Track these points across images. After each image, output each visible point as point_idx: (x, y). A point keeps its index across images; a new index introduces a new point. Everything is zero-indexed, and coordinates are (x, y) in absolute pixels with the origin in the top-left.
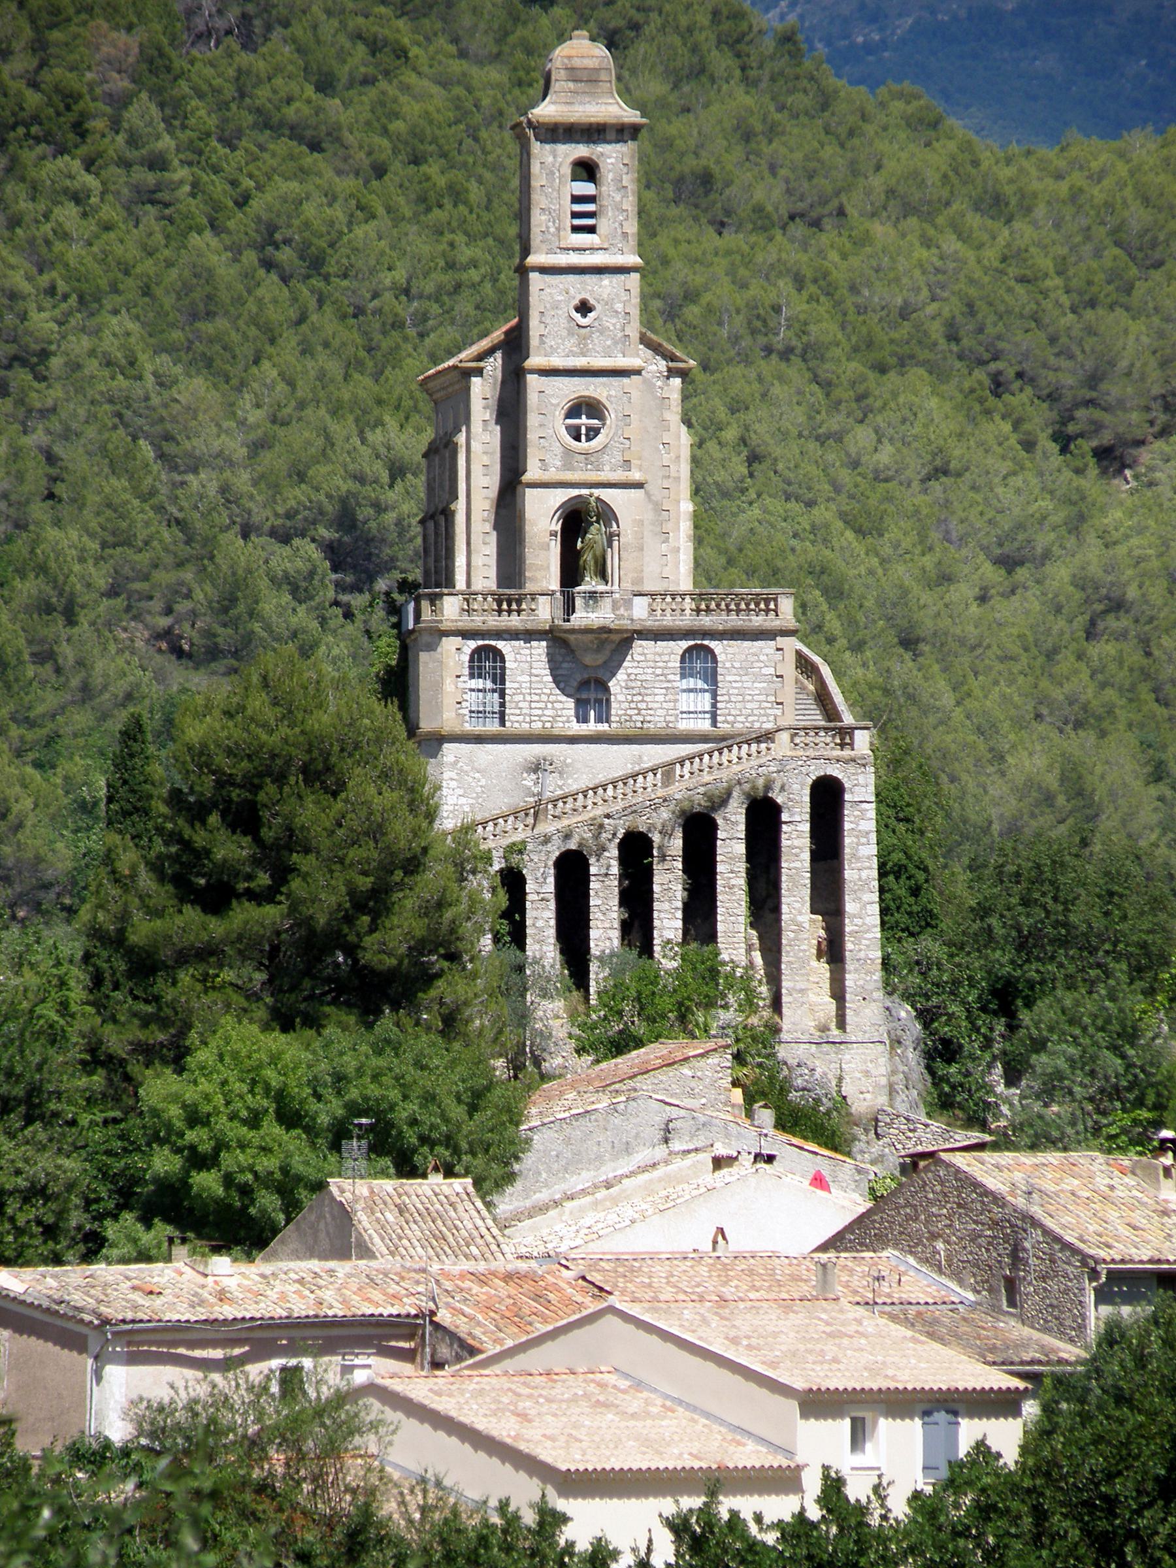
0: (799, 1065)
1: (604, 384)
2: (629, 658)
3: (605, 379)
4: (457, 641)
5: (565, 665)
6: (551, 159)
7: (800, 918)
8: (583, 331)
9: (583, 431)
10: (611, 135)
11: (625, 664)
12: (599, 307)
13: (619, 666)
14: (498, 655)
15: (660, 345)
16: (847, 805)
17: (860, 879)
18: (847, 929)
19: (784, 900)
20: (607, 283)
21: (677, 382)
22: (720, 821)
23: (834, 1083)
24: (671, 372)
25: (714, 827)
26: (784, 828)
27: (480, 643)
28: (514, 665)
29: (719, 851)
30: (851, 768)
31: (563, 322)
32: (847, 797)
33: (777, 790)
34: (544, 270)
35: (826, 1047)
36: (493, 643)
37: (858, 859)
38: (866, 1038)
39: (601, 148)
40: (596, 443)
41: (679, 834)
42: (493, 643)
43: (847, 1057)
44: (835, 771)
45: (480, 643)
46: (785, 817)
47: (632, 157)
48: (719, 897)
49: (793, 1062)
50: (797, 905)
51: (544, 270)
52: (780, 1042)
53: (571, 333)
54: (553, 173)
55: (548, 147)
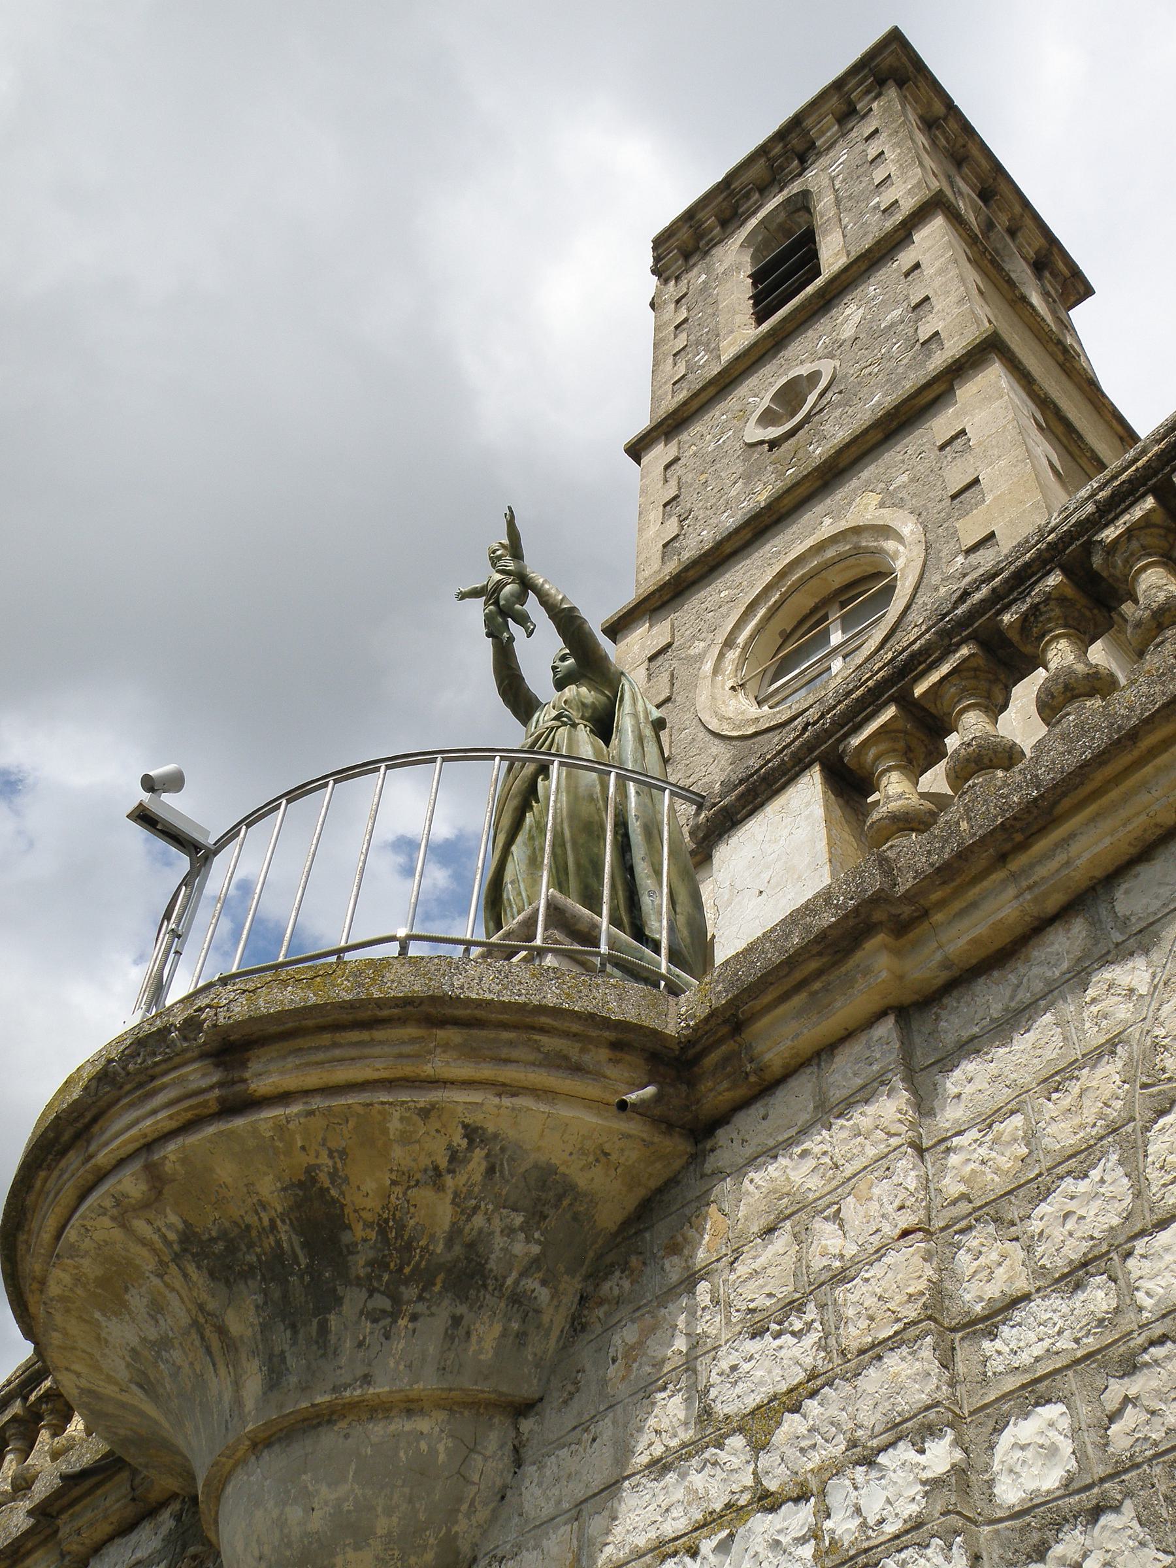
1: (867, 487)
8: (786, 446)
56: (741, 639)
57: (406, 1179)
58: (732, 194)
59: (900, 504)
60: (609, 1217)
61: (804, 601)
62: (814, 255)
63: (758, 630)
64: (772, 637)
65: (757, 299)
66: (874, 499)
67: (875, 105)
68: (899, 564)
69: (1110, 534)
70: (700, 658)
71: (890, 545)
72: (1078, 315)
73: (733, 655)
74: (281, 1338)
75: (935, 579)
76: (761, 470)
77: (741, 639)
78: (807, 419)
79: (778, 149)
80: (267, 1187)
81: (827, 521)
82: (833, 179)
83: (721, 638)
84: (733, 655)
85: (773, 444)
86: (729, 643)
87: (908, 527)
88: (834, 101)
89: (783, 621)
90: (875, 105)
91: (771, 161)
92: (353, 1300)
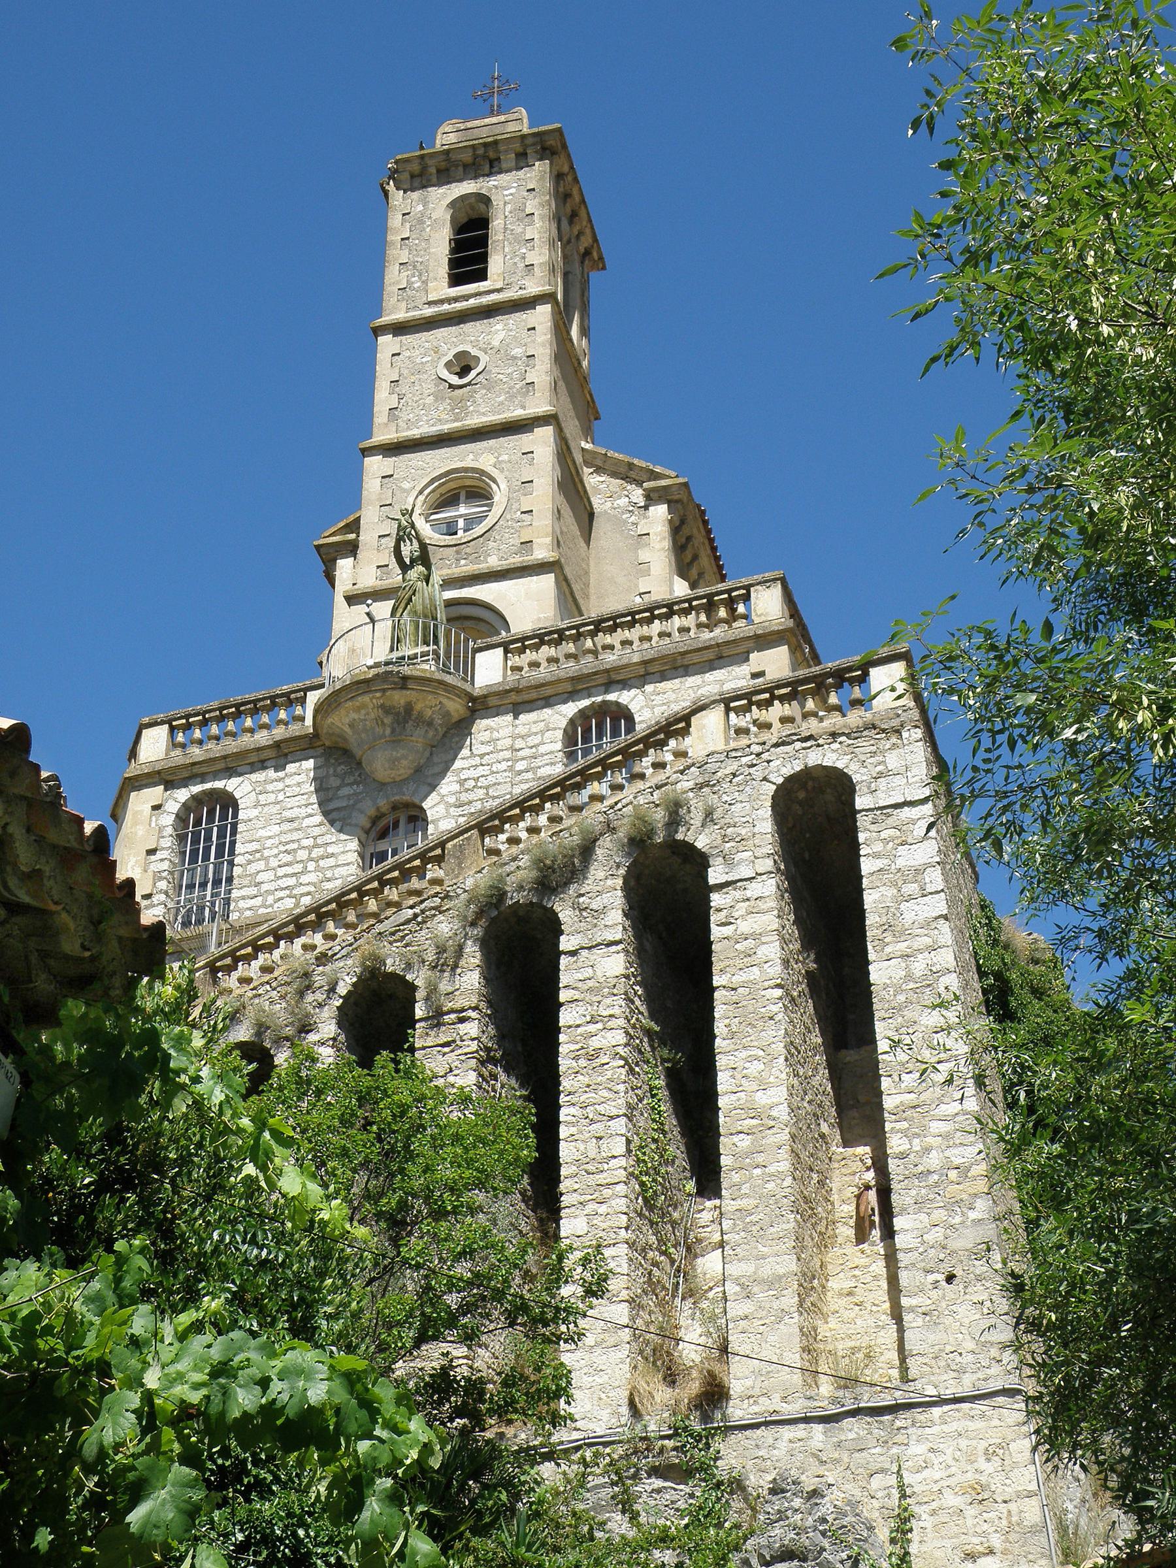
0: (776, 1490)
1: (490, 450)
2: (465, 752)
3: (492, 442)
4: (156, 793)
5: (346, 791)
6: (420, 208)
7: (762, 1099)
9: (461, 523)
10: (509, 159)
11: (458, 764)
12: (484, 359)
13: (447, 769)
14: (228, 803)
15: (631, 466)
16: (862, 821)
17: (909, 977)
18: (889, 1103)
19: (721, 1062)
20: (499, 329)
21: (661, 511)
22: (565, 915)
23: (883, 1533)
24: (652, 498)
25: (554, 928)
26: (716, 899)
27: (196, 789)
28: (253, 813)
29: (564, 979)
30: (865, 746)
31: (429, 387)
32: (860, 802)
33: (696, 818)
34: (400, 329)
35: (853, 1428)
36: (219, 784)
37: (902, 934)
38: (965, 1387)
39: (493, 181)
40: (479, 530)
41: (473, 955)
42: (219, 784)
43: (917, 1449)
44: (830, 757)
45: (196, 789)
46: (715, 876)
47: (542, 178)
48: (566, 1084)
49: (758, 1482)
50: (755, 1068)
51: (400, 329)
52: (729, 1430)
53: (438, 397)
54: (421, 222)
55: (415, 195)
56: (426, 492)
57: (426, 706)
58: (448, 160)
59: (502, 470)
60: (454, 720)
61: (453, 485)
62: (483, 258)
63: (433, 491)
64: (437, 495)
65: (454, 263)
66: (493, 460)
67: (537, 164)
68: (496, 499)
69: (567, 633)
70: (408, 491)
71: (494, 486)
72: (595, 276)
73: (421, 498)
74: (395, 725)
75: (508, 517)
76: (443, 399)
77: (426, 492)
78: (469, 384)
79: (481, 151)
80: (402, 702)
81: (471, 456)
82: (505, 203)
83: (418, 488)
84: (421, 498)
85: (451, 386)
86: (421, 492)
87: (503, 486)
88: (517, 146)
89: (443, 490)
90: (537, 164)
91: (475, 157)
92: (411, 723)
